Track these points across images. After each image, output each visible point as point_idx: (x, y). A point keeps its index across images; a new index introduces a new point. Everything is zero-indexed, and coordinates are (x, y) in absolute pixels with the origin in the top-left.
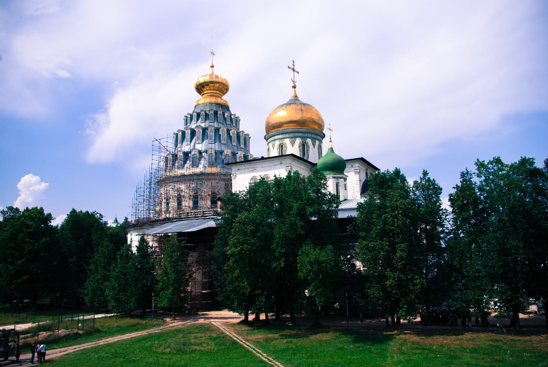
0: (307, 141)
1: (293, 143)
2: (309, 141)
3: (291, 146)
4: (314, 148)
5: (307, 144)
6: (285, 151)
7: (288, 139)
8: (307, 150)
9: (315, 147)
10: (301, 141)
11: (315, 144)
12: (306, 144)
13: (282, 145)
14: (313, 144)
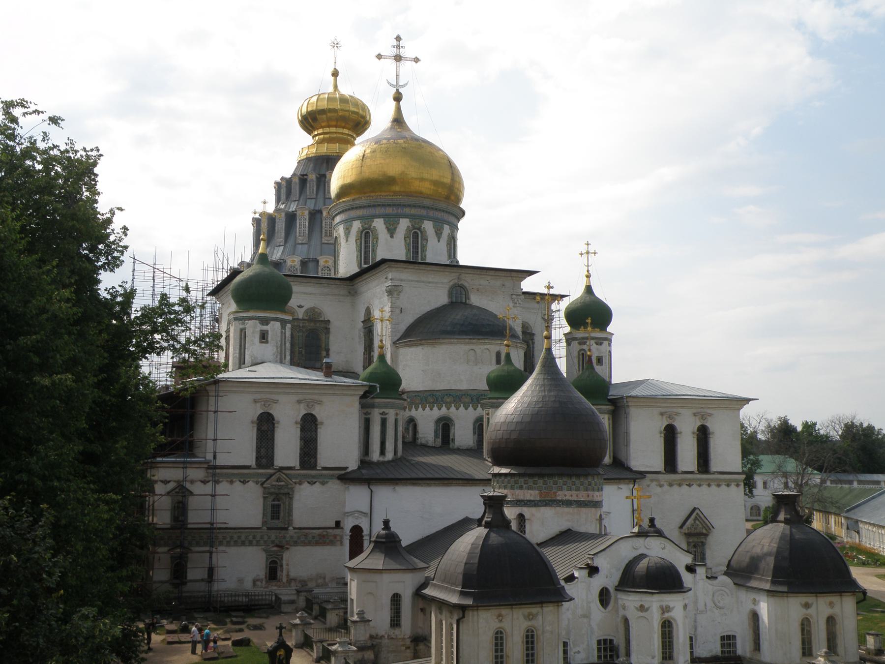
0: (423, 226)
1: (392, 232)
2: (428, 226)
3: (389, 235)
4: (439, 241)
5: (423, 232)
6: (373, 246)
7: (382, 219)
8: (422, 243)
9: (441, 240)
10: (410, 225)
11: (441, 233)
12: (422, 232)
13: (368, 232)
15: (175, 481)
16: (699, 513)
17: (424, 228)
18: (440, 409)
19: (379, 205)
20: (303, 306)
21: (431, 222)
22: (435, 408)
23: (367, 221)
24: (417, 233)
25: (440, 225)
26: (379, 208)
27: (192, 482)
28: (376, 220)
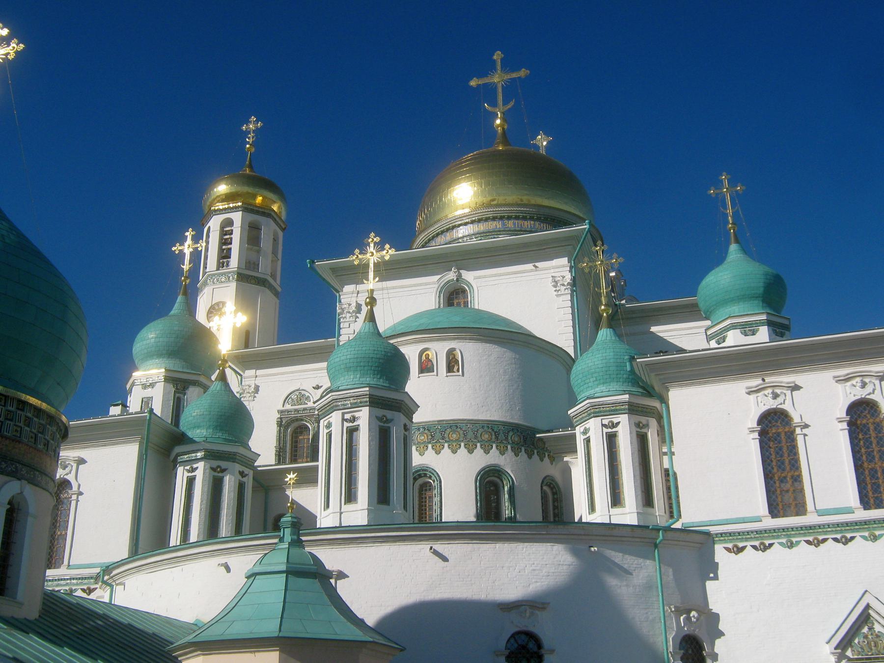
20: (322, 386)
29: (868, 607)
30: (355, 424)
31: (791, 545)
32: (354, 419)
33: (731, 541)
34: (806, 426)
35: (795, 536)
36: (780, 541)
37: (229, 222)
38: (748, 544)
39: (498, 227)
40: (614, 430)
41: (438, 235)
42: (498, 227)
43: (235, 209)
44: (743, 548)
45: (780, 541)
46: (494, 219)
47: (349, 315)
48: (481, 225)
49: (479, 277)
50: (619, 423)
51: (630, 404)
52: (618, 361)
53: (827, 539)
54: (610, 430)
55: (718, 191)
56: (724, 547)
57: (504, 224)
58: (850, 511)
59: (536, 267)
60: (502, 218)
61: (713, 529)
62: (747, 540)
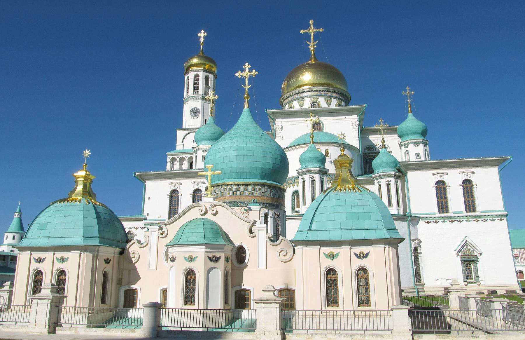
0: (318, 100)
1: (301, 105)
7: (297, 101)
12: (317, 103)
14: (327, 103)
15: (128, 228)
16: (468, 240)
17: (319, 101)
18: (293, 187)
19: (295, 94)
21: (324, 98)
22: (292, 187)
23: (290, 103)
24: (316, 105)
25: (330, 98)
26: (295, 95)
27: (137, 228)
28: (294, 102)
29: (467, 241)
30: (314, 179)
31: (444, 222)
32: (313, 178)
33: (427, 220)
34: (450, 186)
35: (446, 219)
36: (441, 220)
37: (197, 75)
38: (432, 221)
39: (318, 94)
40: (389, 183)
41: (295, 94)
42: (318, 94)
43: (200, 70)
44: (430, 222)
45: (441, 220)
46: (317, 91)
47: (278, 130)
48: (312, 92)
49: (326, 120)
50: (390, 181)
51: (395, 175)
52: (390, 161)
53: (455, 221)
54: (388, 183)
55: (406, 93)
56: (425, 222)
57: (320, 93)
58: (462, 213)
59: (345, 117)
60: (320, 91)
61: (421, 216)
62: (431, 219)
